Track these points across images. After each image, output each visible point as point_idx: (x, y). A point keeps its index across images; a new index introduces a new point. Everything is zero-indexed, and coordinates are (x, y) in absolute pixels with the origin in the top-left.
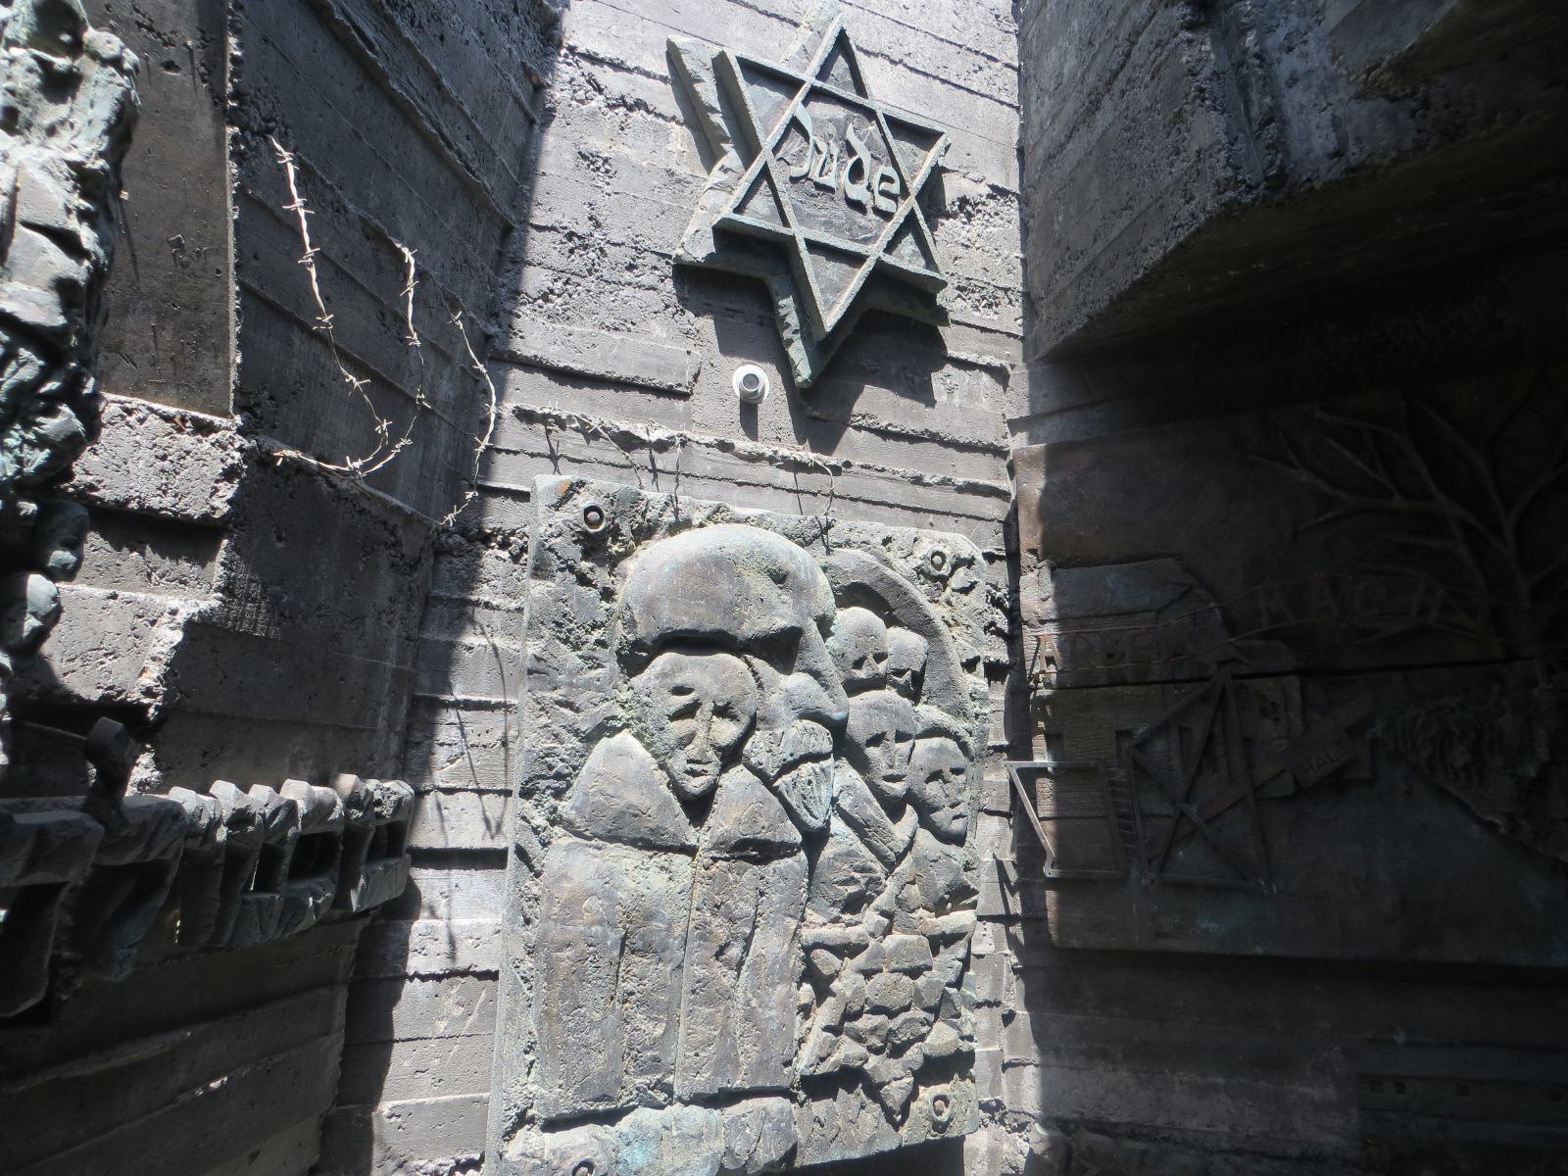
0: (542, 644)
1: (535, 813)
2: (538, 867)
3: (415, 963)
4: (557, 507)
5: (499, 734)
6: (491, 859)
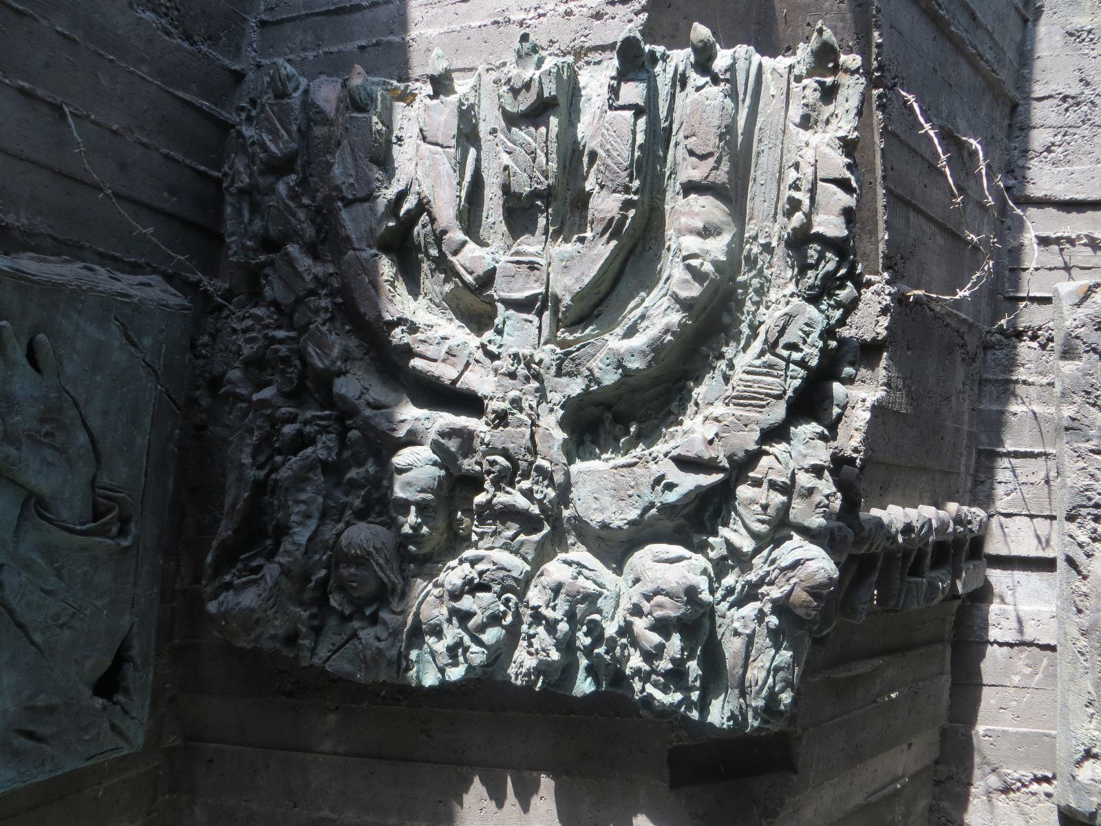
0: (1075, 408)
1: (1078, 532)
2: (1085, 572)
3: (994, 634)
4: (1078, 305)
5: (1043, 474)
6: (1048, 565)
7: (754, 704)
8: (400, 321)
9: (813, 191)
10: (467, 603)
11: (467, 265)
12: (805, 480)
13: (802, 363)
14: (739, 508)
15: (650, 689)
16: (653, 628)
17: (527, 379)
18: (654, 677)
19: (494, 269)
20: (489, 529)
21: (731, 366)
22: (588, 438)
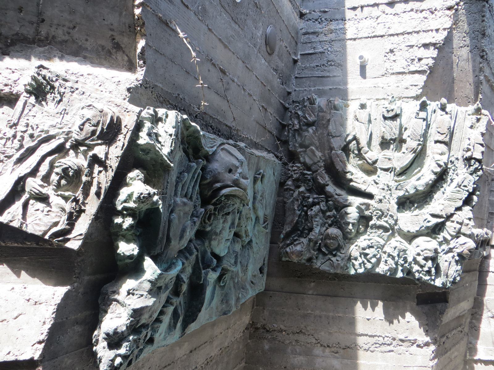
7: (450, 280)
8: (349, 172)
9: (474, 146)
10: (367, 251)
11: (370, 157)
12: (466, 221)
13: (468, 191)
14: (447, 228)
15: (421, 275)
16: (423, 259)
17: (387, 190)
18: (422, 272)
19: (378, 159)
20: (373, 231)
21: (445, 190)
22: (401, 207)
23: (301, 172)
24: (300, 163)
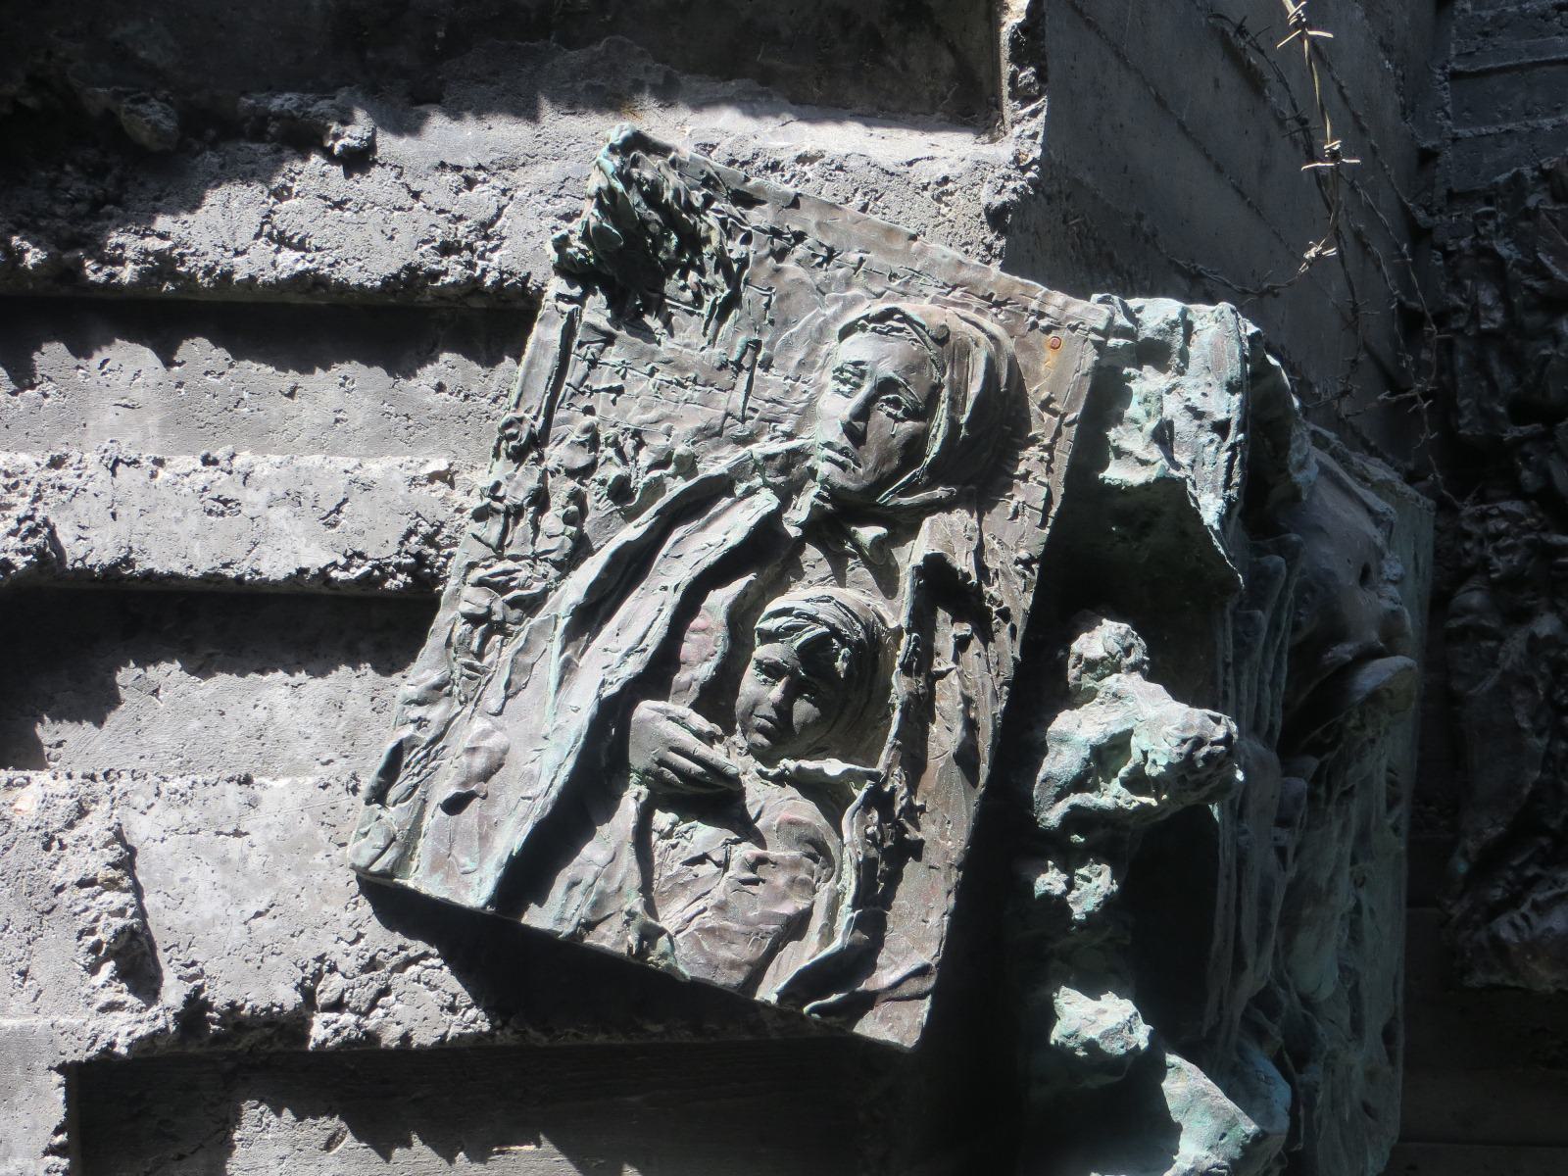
23: (1530, 544)
24: (1518, 493)
